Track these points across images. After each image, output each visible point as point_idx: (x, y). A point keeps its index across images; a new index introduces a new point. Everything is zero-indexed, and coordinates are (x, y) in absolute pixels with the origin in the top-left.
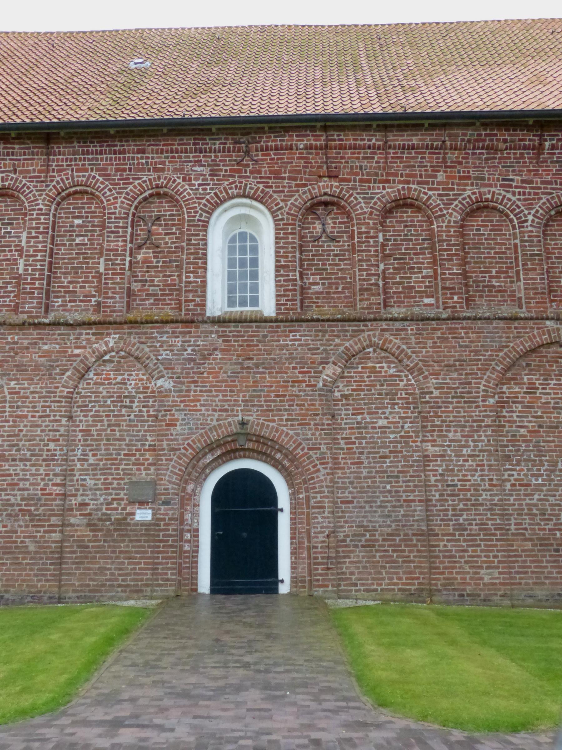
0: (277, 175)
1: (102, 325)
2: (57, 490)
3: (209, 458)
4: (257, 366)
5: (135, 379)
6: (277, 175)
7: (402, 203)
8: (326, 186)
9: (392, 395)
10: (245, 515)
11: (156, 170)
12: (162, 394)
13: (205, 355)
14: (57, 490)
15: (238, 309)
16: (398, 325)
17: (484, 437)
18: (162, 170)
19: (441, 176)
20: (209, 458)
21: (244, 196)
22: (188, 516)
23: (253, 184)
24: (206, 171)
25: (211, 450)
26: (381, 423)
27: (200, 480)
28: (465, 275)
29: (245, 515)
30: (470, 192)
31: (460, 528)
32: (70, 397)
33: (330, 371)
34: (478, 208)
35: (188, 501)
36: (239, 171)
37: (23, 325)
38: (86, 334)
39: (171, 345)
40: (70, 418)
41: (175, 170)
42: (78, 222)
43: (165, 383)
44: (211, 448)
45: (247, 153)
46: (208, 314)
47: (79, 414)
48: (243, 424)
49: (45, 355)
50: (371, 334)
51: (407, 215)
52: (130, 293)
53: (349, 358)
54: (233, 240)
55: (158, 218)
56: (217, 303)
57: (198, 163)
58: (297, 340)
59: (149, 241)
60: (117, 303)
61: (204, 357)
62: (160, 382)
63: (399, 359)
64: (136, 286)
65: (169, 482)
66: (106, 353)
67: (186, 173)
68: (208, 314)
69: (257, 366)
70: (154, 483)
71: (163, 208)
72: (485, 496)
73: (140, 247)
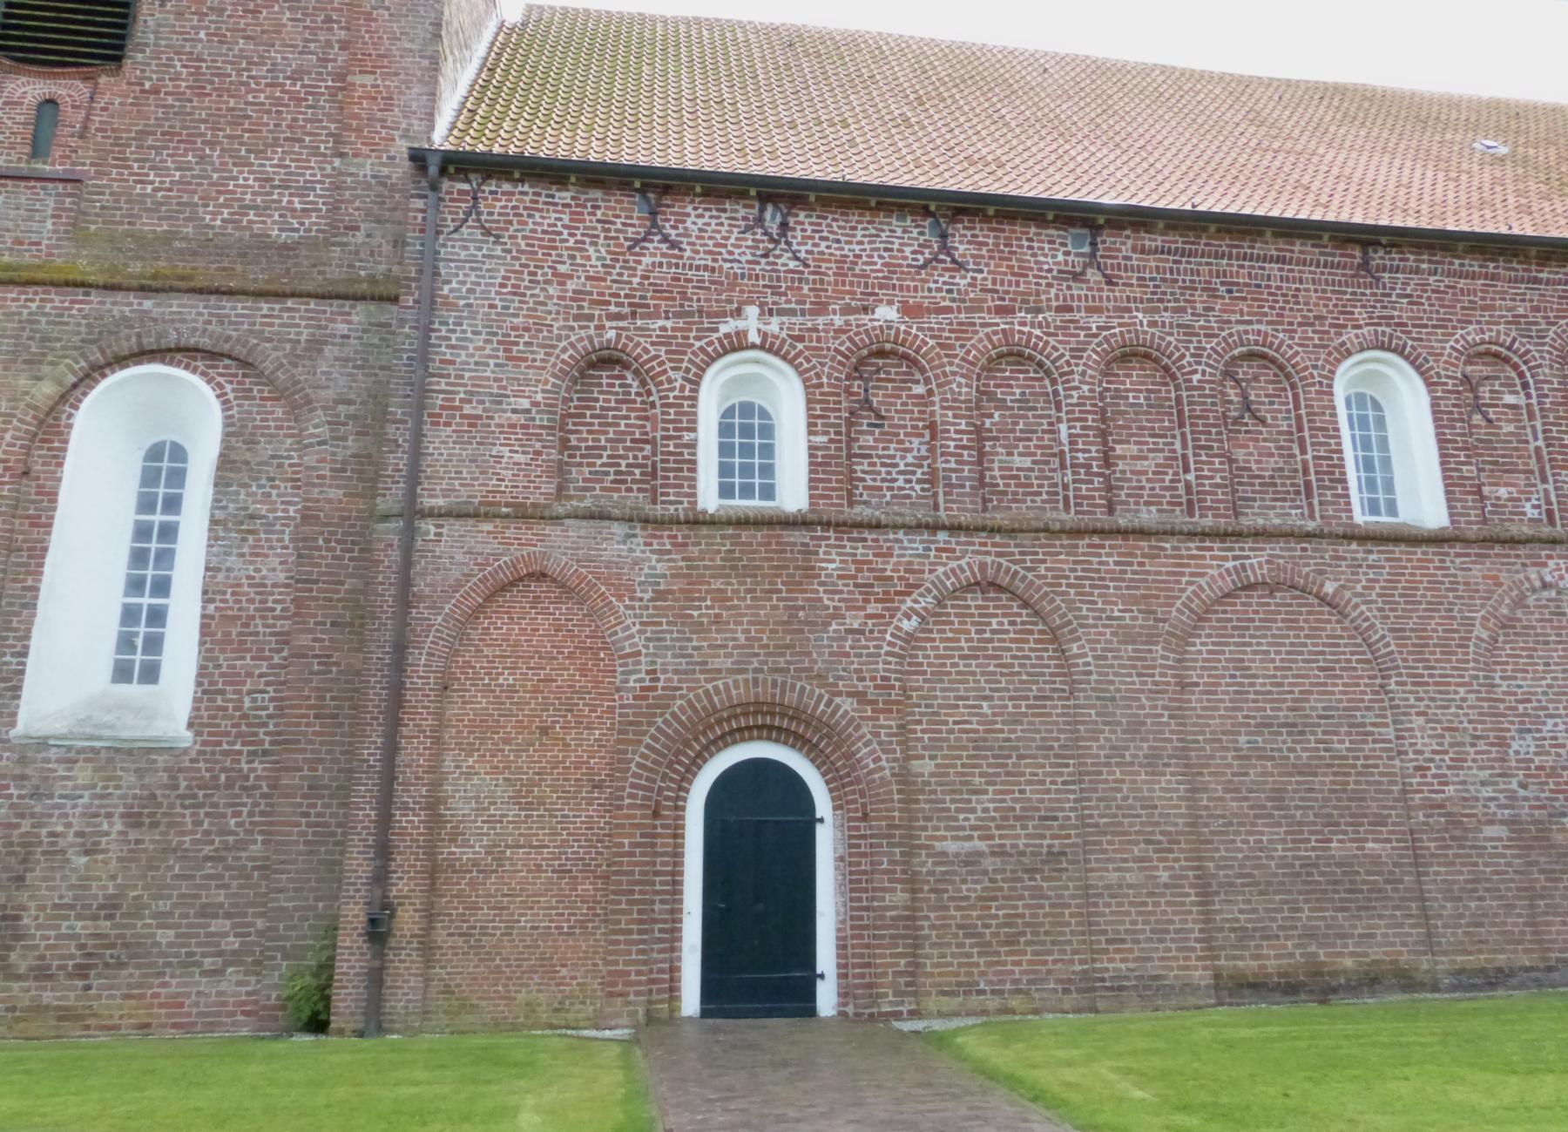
10: (760, 845)
29: (760, 845)
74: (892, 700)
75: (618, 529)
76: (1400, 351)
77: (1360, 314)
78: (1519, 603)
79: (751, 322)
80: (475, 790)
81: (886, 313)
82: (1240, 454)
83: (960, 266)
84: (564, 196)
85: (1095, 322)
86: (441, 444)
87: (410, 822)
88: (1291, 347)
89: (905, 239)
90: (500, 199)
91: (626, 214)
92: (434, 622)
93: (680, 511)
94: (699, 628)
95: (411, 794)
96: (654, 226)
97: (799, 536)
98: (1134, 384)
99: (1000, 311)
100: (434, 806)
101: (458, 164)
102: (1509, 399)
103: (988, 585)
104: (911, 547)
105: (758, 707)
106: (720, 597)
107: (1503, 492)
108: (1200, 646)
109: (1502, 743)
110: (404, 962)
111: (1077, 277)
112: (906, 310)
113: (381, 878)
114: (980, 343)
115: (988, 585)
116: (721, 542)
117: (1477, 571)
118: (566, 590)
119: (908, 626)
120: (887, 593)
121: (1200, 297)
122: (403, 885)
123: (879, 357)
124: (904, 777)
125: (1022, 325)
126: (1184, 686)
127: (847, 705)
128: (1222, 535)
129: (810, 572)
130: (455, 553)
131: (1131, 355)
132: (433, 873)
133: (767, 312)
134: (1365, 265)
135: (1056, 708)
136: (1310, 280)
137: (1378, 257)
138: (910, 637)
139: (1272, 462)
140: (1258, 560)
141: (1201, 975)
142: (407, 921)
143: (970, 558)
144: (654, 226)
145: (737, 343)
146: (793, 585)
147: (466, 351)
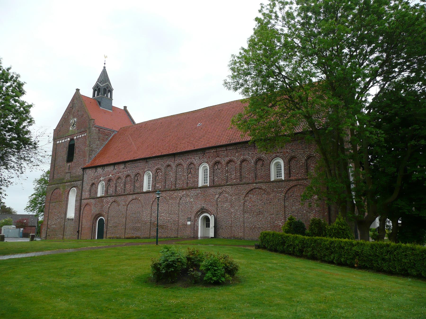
0: (209, 157)
1: (183, 189)
2: (177, 219)
5: (188, 199)
6: (209, 157)
7: (230, 161)
8: (218, 159)
9: (227, 200)
12: (191, 202)
14: (177, 219)
16: (228, 187)
17: (242, 208)
19: (237, 154)
24: (198, 158)
26: (225, 206)
27: (198, 216)
28: (241, 175)
30: (242, 157)
31: (236, 225)
32: (179, 203)
33: (217, 196)
34: (243, 161)
39: (193, 193)
43: (192, 200)
44: (199, 211)
45: (204, 154)
50: (224, 188)
51: (232, 163)
53: (220, 194)
58: (212, 190)
59: (190, 172)
63: (228, 193)
64: (188, 182)
65: (193, 217)
67: (195, 159)
71: (192, 166)
72: (241, 219)
79: (102, 179)
80: (84, 221)
81: (111, 175)
86: (83, 194)
87: (80, 224)
88: (140, 172)
89: (112, 168)
91: (94, 170)
92: (82, 208)
95: (81, 222)
97: (103, 198)
98: (128, 179)
101: (84, 169)
103: (114, 202)
104: (109, 198)
105: (99, 214)
108: (129, 206)
109: (151, 214)
110: (80, 234)
111: (124, 168)
112: (112, 175)
113: (79, 228)
115: (114, 202)
116: (98, 199)
118: (90, 205)
120: (108, 203)
122: (80, 229)
125: (120, 174)
130: (84, 202)
131: (128, 176)
135: (118, 213)
136: (141, 164)
137: (148, 160)
140: (134, 196)
143: (113, 199)
147: (85, 184)
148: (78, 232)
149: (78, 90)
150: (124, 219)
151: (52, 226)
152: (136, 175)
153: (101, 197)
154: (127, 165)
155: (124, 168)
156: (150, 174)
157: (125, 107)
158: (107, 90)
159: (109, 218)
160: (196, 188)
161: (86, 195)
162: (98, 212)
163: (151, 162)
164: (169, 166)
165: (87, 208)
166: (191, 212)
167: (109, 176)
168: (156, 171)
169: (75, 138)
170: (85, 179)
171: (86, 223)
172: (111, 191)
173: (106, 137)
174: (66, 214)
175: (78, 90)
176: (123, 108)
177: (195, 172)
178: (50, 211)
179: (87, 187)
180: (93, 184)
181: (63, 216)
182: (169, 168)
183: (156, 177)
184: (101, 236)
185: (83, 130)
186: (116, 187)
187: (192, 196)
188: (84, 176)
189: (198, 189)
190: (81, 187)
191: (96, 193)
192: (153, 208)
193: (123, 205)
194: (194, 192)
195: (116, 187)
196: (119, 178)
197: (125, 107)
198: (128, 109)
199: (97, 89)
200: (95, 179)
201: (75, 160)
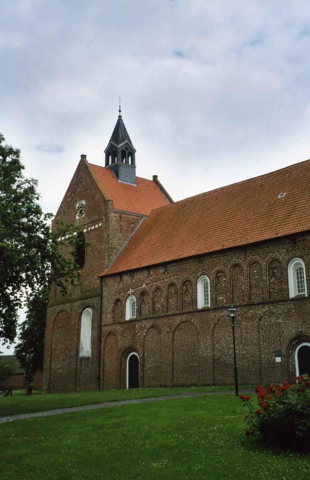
1: (263, 304)
3: (294, 343)
4: (304, 313)
5: (273, 319)
6: (304, 249)
11: (272, 252)
12: (279, 324)
13: (290, 310)
15: (301, 293)
18: (273, 252)
20: (294, 343)
21: (296, 257)
22: (291, 361)
23: (298, 253)
25: (295, 340)
27: (294, 349)
32: (258, 326)
35: (291, 356)
36: (294, 249)
37: (245, 306)
38: (260, 307)
39: (280, 308)
40: (259, 332)
41: (277, 252)
42: (255, 271)
43: (280, 320)
44: (294, 339)
45: (295, 243)
46: (290, 298)
47: (260, 330)
48: (301, 332)
49: (251, 313)
52: (270, 293)
54: (297, 270)
55: (275, 267)
56: (292, 294)
57: (283, 248)
59: (274, 275)
60: (266, 296)
61: (290, 312)
62: (279, 320)
64: (271, 290)
65: (284, 350)
66: (266, 312)
68: (290, 298)
69: (304, 313)
70: (280, 351)
73: (272, 277)
74: (143, 345)
75: (118, 325)
76: (206, 274)
77: (200, 269)
78: (219, 320)
79: (131, 291)
80: (107, 360)
81: (144, 285)
82: (185, 299)
83: (151, 276)
84: (113, 278)
85: (167, 280)
86: (104, 316)
87: (102, 365)
89: (145, 273)
90: (108, 280)
91: (118, 279)
92: (103, 340)
93: (123, 321)
94: (125, 337)
96: (121, 279)
97: (134, 323)
98: (172, 290)
99: (156, 282)
100: (104, 363)
101: (102, 278)
102: (224, 279)
104: (144, 322)
106: (127, 332)
107: (221, 298)
108: (176, 333)
109: (214, 345)
110: (102, 382)
111: (164, 273)
112: (146, 284)
114: (154, 288)
116: (126, 325)
117: (213, 314)
118: (114, 334)
119: (144, 334)
120: (141, 329)
121: (179, 272)
122: (101, 374)
123: (143, 293)
124: (144, 356)
125: (158, 283)
126: (173, 340)
127: (138, 346)
128: (179, 314)
129: (135, 327)
130: (106, 330)
131: (172, 285)
132: (104, 372)
133: (132, 289)
134: (200, 260)
136: (191, 266)
137: (202, 259)
138: (145, 336)
139: (189, 299)
140: (184, 318)
141: (171, 385)
142: (102, 378)
143: (150, 323)
144: (121, 279)
145: (129, 295)
146: (134, 330)
147: (105, 302)
148: (99, 378)
149: (83, 157)
150: (170, 355)
151: (58, 371)
152: (184, 284)
153: (131, 321)
154: (169, 267)
155: (164, 273)
156: (205, 279)
157: (155, 177)
158: (127, 152)
159: (146, 354)
160: (286, 300)
161: (108, 318)
162: (127, 345)
163: (207, 262)
164: (236, 265)
165: (111, 339)
166: (280, 340)
167: (141, 287)
168: (217, 276)
169: (85, 231)
170: (105, 293)
171: (110, 363)
172: (146, 309)
173: (132, 226)
174: (77, 351)
175: (83, 157)
176: (151, 179)
177: (282, 273)
178: (53, 346)
179: (108, 306)
180: (118, 300)
181: (73, 353)
182: (237, 269)
183: (216, 284)
184: (134, 384)
185: (96, 217)
186: (154, 304)
187: (280, 314)
188: (104, 289)
189: (289, 302)
190: (98, 307)
191: (124, 314)
192: (215, 335)
193: (167, 332)
194: (283, 307)
195: (154, 304)
196: (158, 289)
197: (155, 177)
198: (159, 179)
199: (111, 152)
200: (120, 292)
201: (87, 265)
